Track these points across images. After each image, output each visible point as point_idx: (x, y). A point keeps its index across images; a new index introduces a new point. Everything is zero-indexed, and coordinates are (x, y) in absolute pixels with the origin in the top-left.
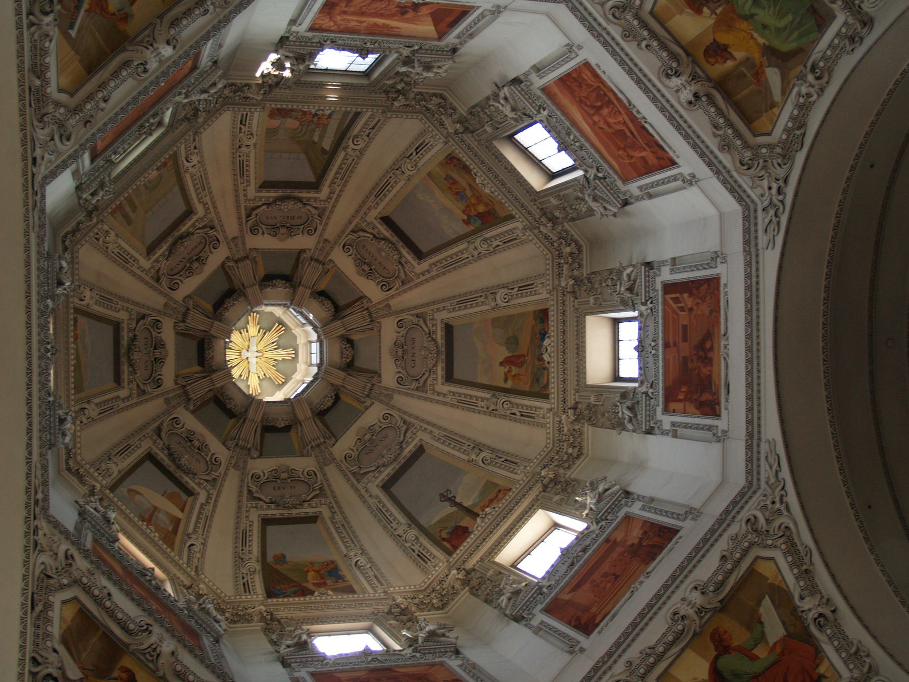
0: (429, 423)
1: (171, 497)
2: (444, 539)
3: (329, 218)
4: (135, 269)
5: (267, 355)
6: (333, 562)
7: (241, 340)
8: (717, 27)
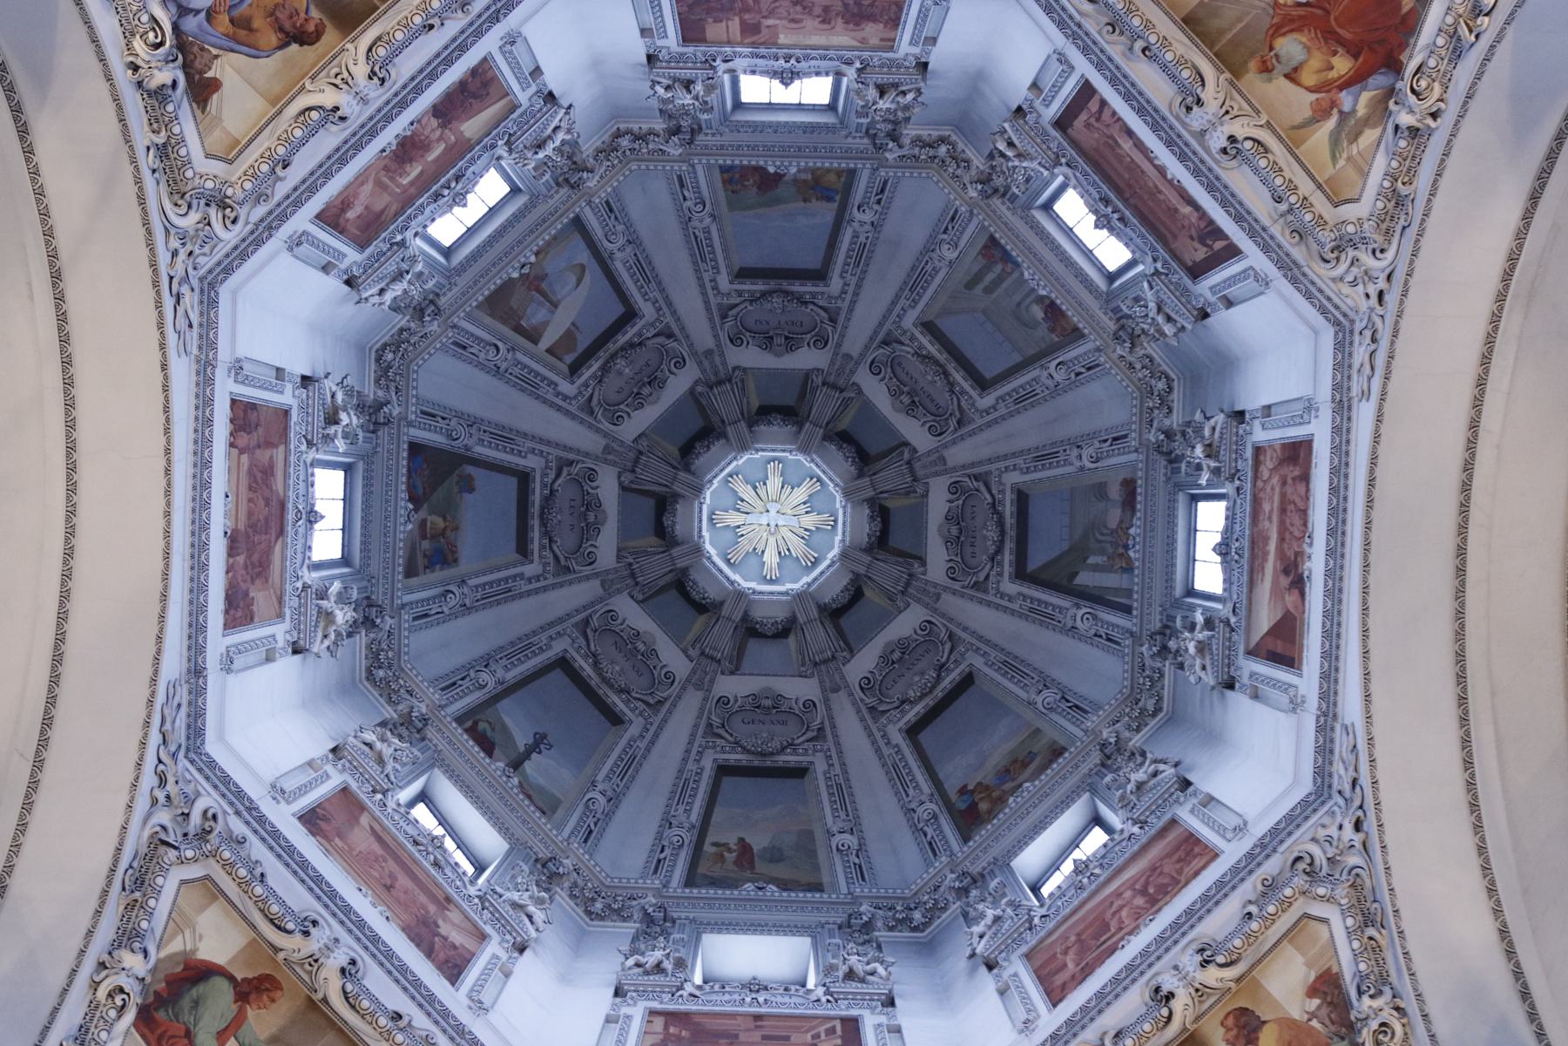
0: (656, 735)
1: (569, 337)
2: (476, 723)
3: (972, 598)
4: (902, 302)
5: (772, 540)
6: (456, 561)
7: (795, 503)
8: (1288, 1023)
